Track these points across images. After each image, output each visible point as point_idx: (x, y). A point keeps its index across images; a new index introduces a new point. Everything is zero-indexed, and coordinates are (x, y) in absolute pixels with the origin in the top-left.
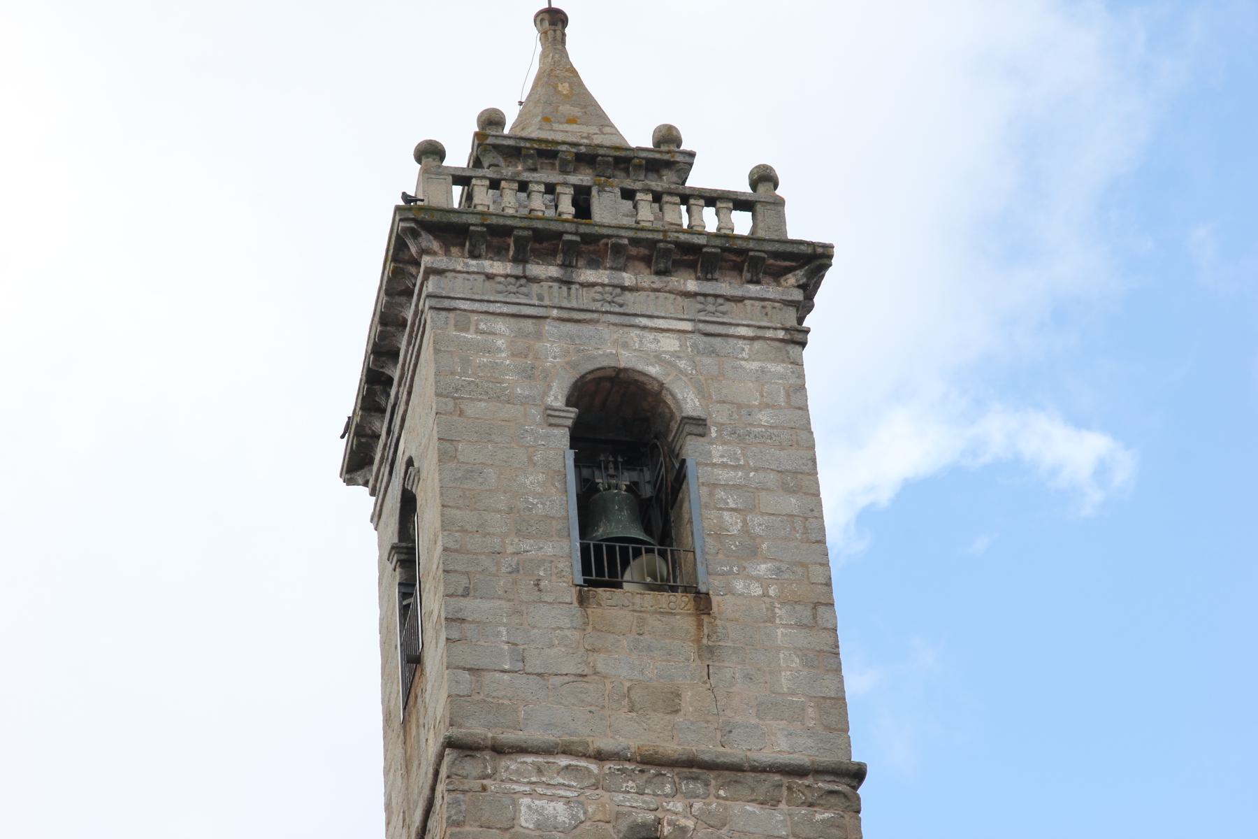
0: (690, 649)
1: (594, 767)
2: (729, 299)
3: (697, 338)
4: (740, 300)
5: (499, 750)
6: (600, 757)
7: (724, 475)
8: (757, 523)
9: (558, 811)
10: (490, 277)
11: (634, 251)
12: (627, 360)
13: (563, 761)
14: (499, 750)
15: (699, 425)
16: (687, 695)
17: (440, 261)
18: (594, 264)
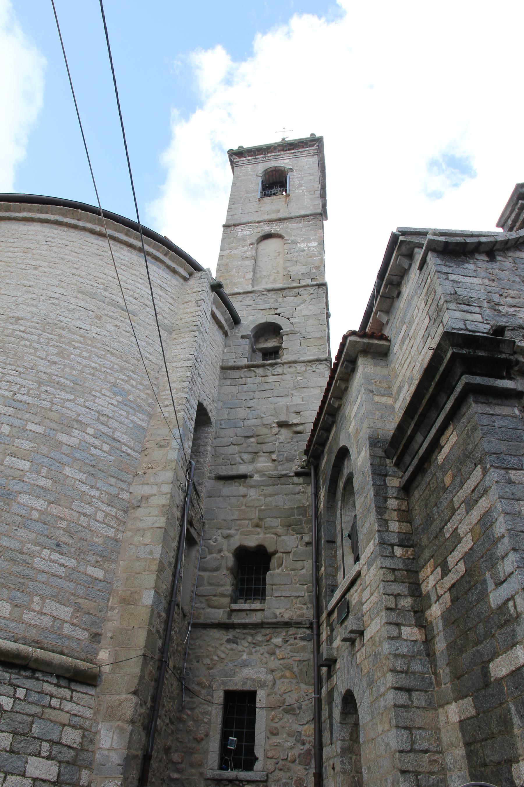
0: (283, 203)
1: (257, 225)
2: (301, 152)
3: (294, 159)
4: (304, 151)
5: (235, 225)
6: (258, 222)
7: (295, 176)
8: (302, 182)
9: (248, 233)
10: (248, 160)
11: (280, 149)
12: (276, 165)
13: (250, 225)
14: (235, 225)
15: (291, 170)
16: (281, 210)
17: (238, 160)
18: (272, 152)
